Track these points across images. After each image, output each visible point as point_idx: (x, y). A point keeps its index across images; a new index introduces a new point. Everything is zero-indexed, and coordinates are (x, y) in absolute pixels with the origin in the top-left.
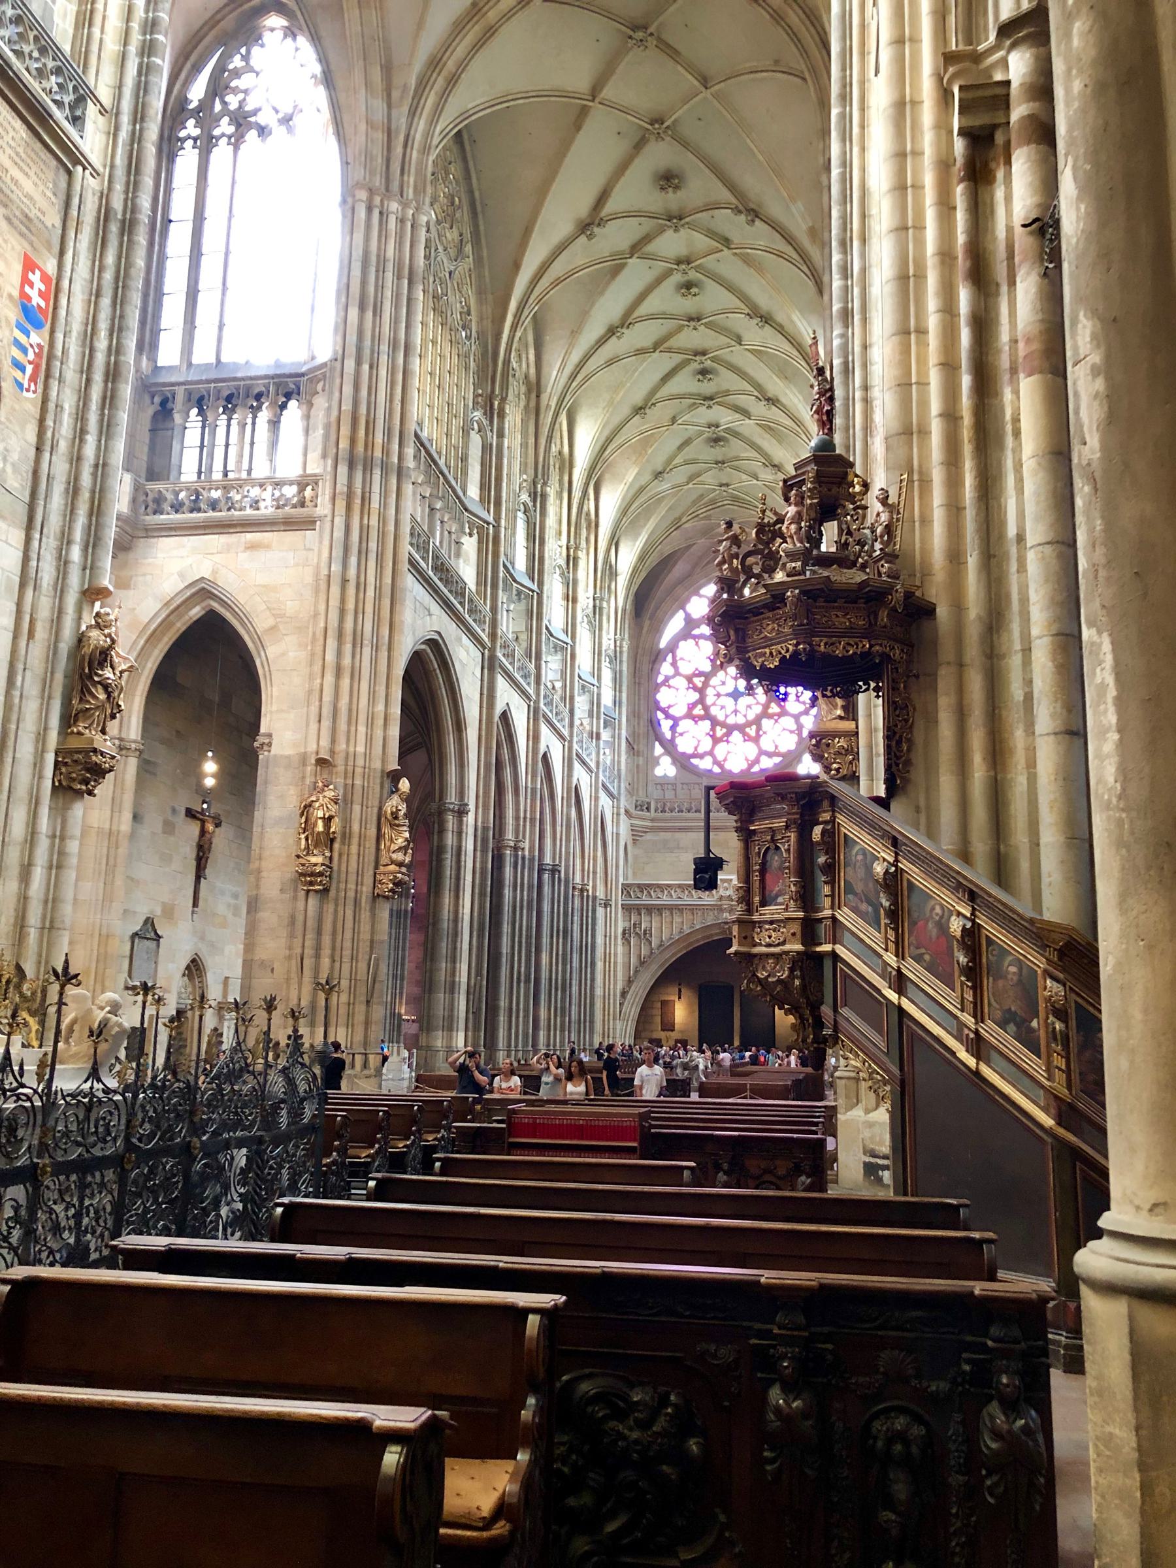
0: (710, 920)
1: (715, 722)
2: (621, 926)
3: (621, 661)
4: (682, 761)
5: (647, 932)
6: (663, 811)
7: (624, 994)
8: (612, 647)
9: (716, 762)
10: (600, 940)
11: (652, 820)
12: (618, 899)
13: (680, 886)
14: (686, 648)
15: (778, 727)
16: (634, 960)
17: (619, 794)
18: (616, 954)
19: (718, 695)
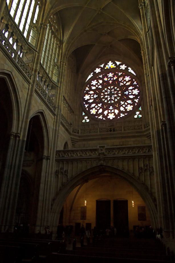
0: (94, 165)
1: (103, 104)
2: (54, 169)
3: (62, 69)
4: (92, 117)
5: (66, 171)
6: (84, 133)
7: (54, 200)
8: (59, 64)
9: (104, 116)
10: (43, 174)
11: (79, 137)
12: (53, 157)
13: (81, 151)
14: (94, 83)
15: (126, 104)
16: (59, 185)
17: (58, 114)
18: (51, 181)
19: (105, 95)
